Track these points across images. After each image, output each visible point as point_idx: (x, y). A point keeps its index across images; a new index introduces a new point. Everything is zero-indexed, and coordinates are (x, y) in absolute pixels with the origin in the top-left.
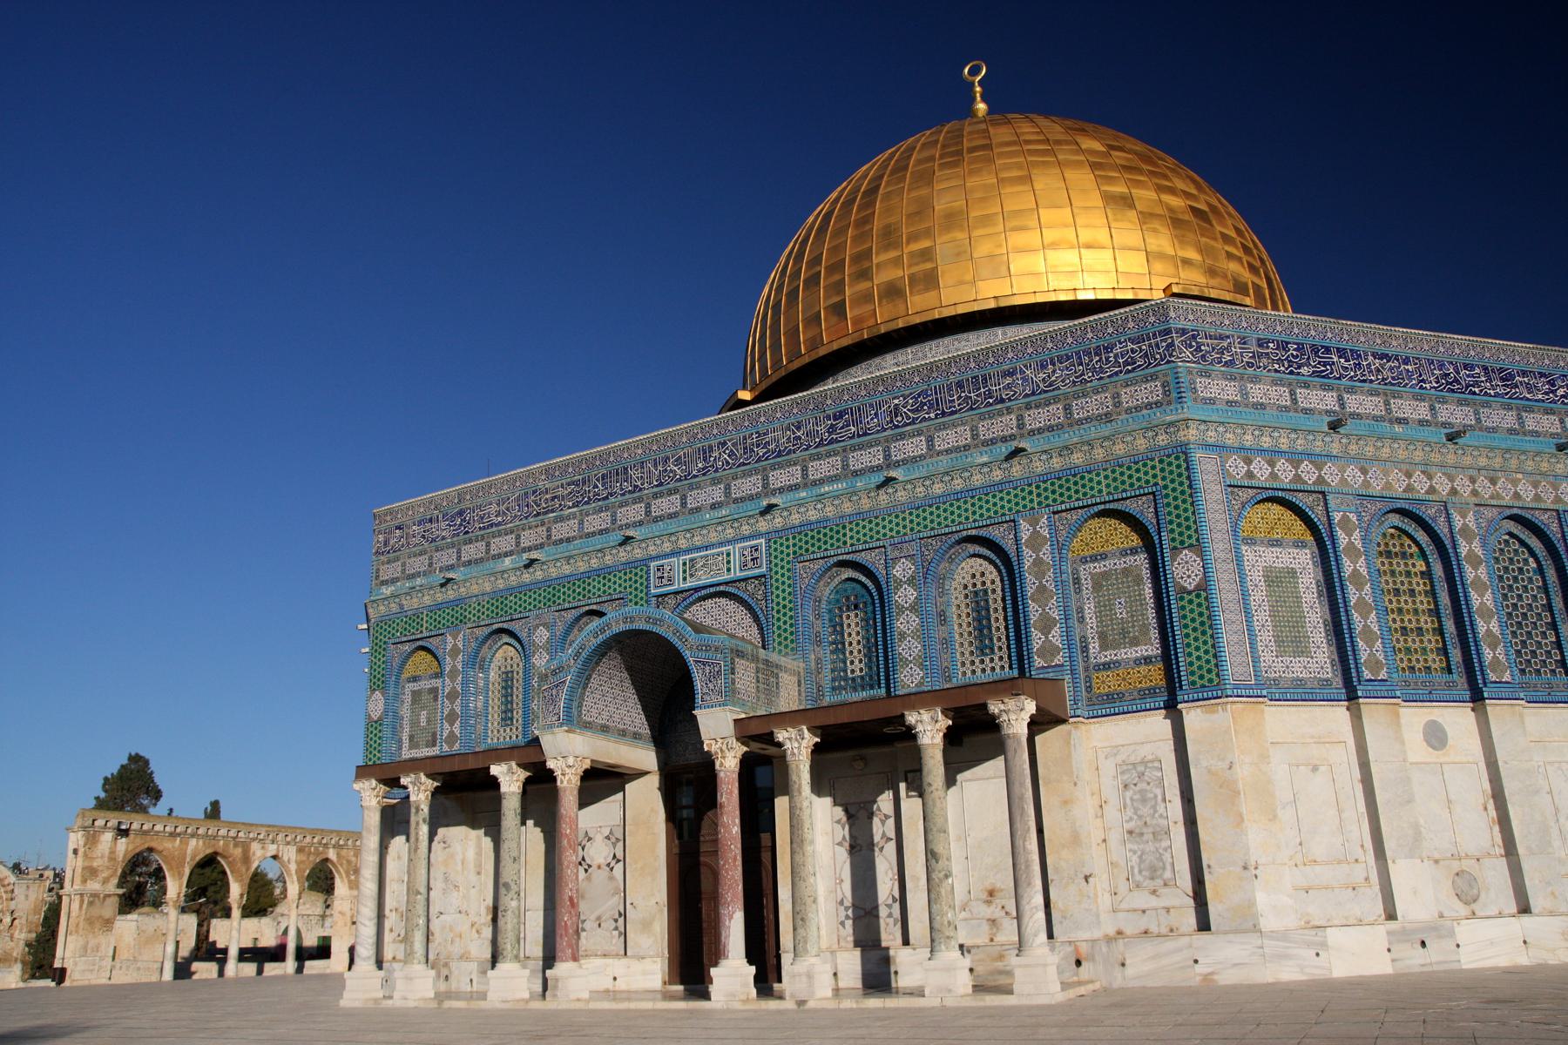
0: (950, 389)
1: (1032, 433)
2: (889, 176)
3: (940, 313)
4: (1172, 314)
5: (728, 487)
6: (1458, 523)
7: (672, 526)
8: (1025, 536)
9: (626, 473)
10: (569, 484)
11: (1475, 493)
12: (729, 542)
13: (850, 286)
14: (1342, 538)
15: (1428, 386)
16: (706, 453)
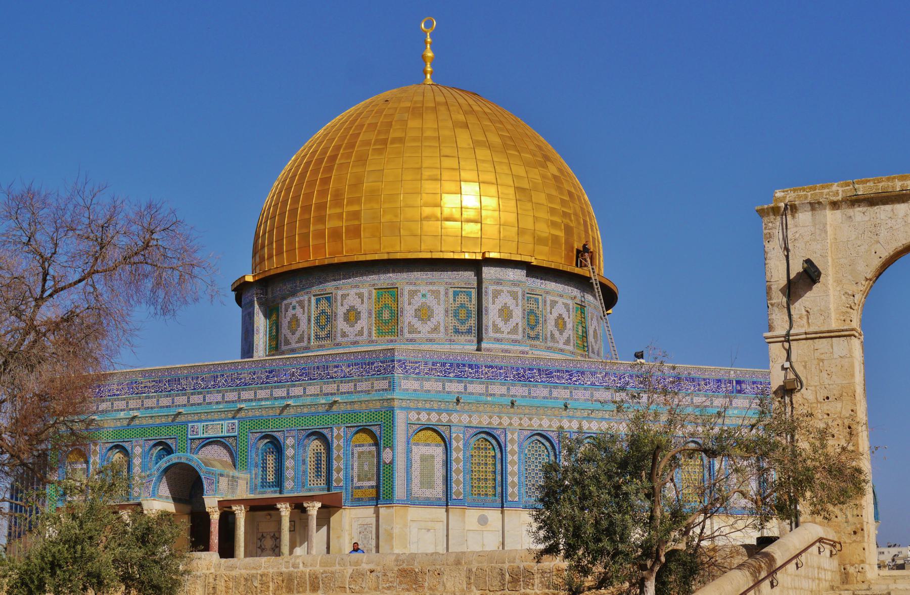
0: (314, 369)
1: (342, 393)
2: (345, 149)
3: (357, 258)
4: (396, 354)
5: (223, 395)
6: (509, 436)
7: (199, 409)
8: (335, 435)
9: (179, 381)
10: (154, 381)
11: (520, 424)
12: (223, 420)
13: (313, 225)
14: (454, 444)
15: (509, 379)
16: (215, 378)
